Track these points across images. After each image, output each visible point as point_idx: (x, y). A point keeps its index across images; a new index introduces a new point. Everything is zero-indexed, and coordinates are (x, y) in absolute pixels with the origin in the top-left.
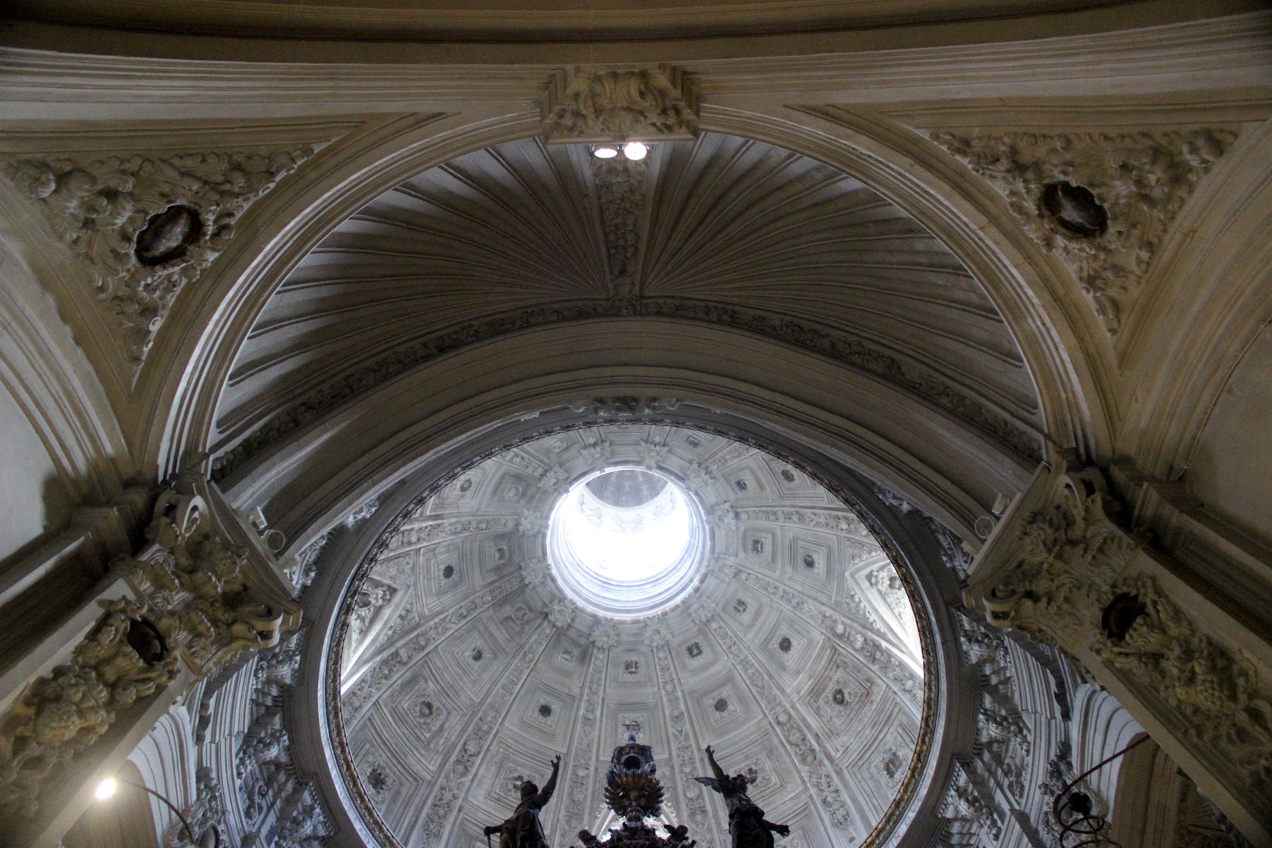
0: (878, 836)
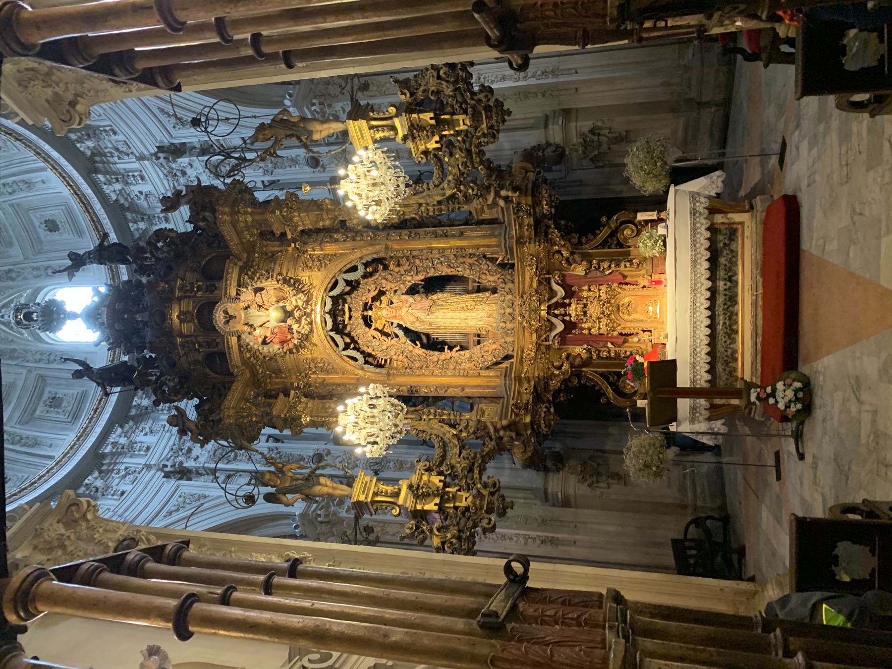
0: (56, 170)
